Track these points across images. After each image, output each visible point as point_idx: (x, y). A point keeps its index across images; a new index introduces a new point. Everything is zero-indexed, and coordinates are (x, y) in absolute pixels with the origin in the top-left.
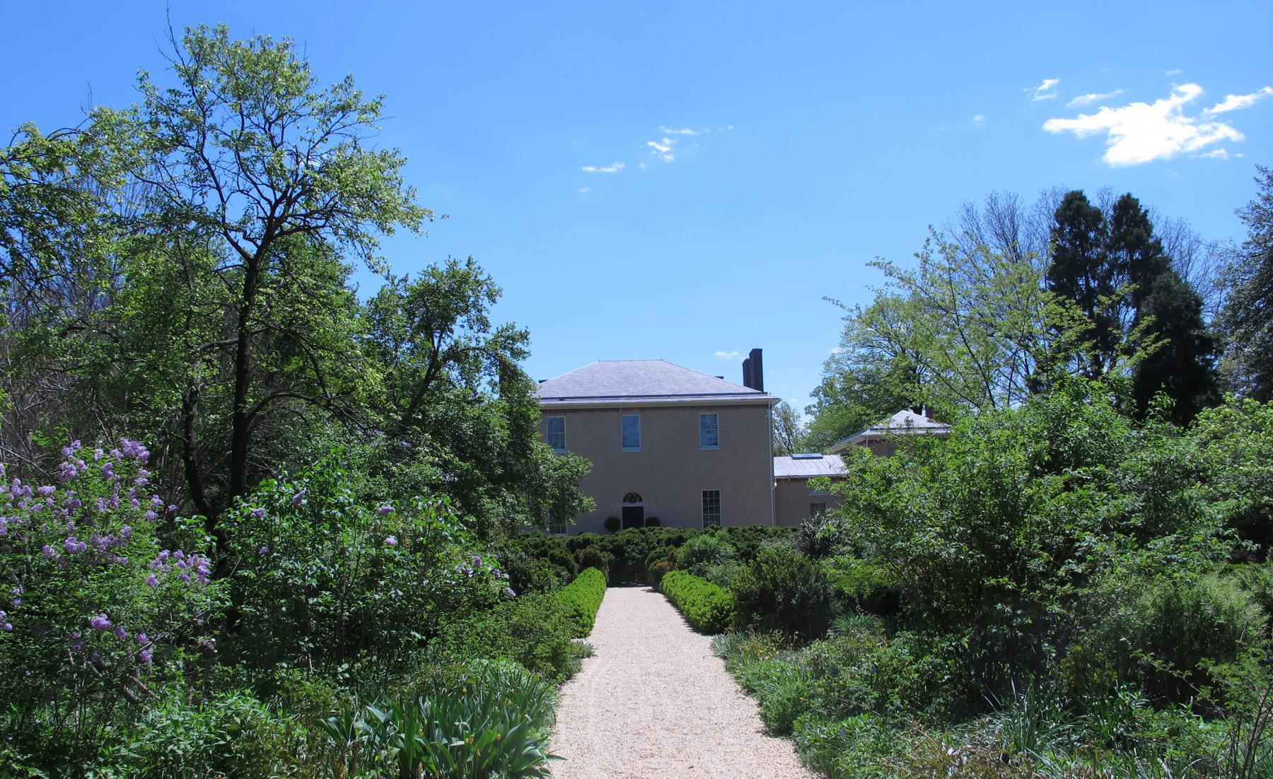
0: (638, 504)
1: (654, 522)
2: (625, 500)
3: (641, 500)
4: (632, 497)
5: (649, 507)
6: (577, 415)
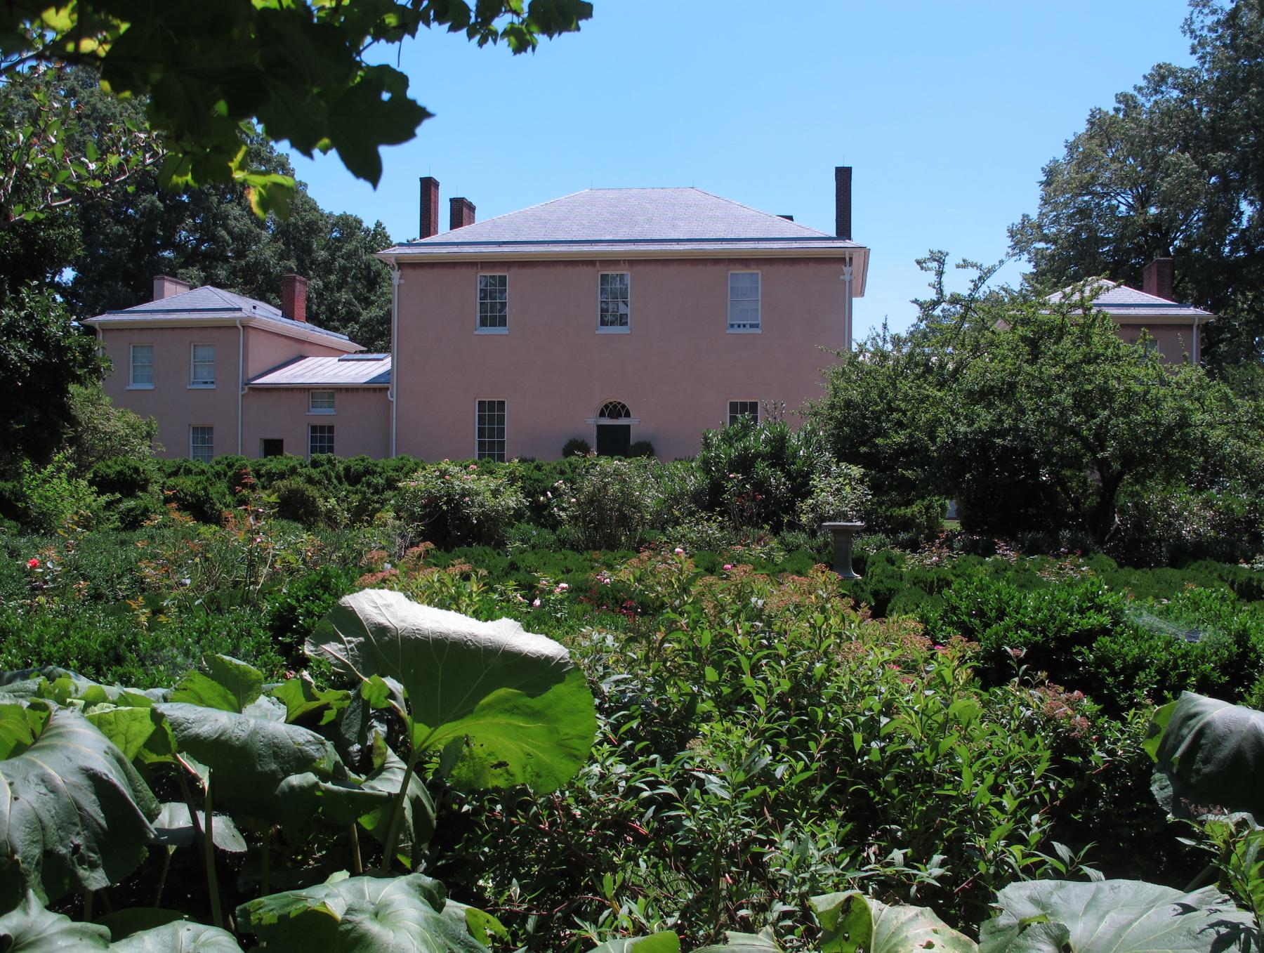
0: (622, 421)
1: (645, 449)
2: (602, 414)
3: (628, 415)
4: (615, 410)
5: (638, 425)
6: (526, 271)
